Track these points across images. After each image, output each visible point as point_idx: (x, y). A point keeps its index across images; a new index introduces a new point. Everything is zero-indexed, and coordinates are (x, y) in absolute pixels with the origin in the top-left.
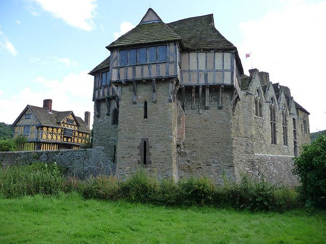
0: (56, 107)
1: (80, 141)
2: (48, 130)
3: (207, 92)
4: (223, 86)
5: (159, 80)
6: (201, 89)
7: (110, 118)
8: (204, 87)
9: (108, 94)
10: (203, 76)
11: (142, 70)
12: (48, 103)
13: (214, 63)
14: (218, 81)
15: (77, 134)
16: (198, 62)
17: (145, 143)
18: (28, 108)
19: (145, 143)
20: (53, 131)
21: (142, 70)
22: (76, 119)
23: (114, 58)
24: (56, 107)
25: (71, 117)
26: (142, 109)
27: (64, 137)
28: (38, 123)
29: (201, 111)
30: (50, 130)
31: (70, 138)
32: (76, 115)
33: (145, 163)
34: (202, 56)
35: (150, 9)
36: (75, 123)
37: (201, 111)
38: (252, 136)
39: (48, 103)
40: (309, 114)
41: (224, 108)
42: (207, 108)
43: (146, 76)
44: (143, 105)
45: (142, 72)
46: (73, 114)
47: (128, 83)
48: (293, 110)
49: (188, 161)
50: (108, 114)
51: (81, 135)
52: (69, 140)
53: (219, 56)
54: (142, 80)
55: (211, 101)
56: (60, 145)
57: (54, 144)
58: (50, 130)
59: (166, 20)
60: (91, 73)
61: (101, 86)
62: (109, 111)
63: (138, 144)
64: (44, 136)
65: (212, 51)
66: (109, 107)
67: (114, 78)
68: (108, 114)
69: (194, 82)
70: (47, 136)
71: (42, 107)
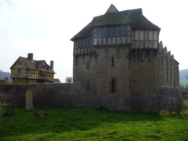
1: (49, 78)
2: (32, 71)
3: (144, 52)
4: (153, 49)
5: (121, 46)
6: (141, 50)
8: (143, 50)
9: (84, 52)
10: (142, 44)
11: (112, 39)
12: (30, 56)
13: (148, 37)
14: (150, 47)
15: (47, 74)
16: (139, 36)
17: (113, 80)
19: (113, 80)
20: (35, 72)
21: (112, 39)
22: (47, 65)
23: (95, 32)
24: (36, 58)
25: (44, 64)
26: (111, 61)
27: (41, 75)
28: (26, 67)
29: (139, 63)
30: (33, 71)
31: (44, 76)
32: (47, 63)
34: (142, 33)
35: (112, 5)
37: (139, 63)
38: (160, 76)
39: (30, 56)
40: (179, 64)
42: (142, 61)
43: (114, 43)
44: (111, 59)
45: (112, 41)
47: (103, 46)
48: (174, 63)
49: (133, 90)
50: (83, 64)
51: (51, 75)
52: (43, 77)
53: (151, 33)
54: (111, 45)
55: (144, 57)
58: (33, 71)
59: (119, 11)
60: (72, 40)
61: (79, 47)
62: (84, 62)
63: (109, 80)
64: (30, 75)
65: (147, 30)
66: (84, 59)
67: (95, 43)
68: (83, 64)
69: (137, 47)
70: (32, 75)
71: (27, 57)
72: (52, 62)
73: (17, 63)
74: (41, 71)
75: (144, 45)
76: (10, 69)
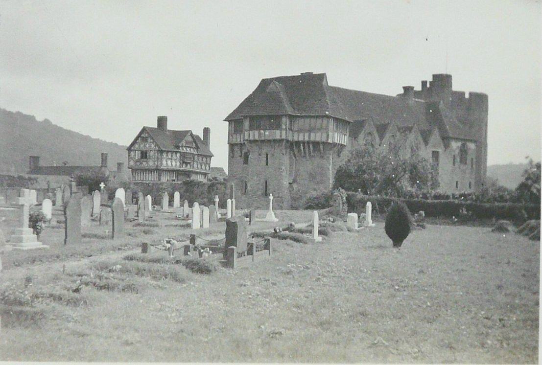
0: (171, 126)
2: (167, 156)
7: (242, 160)
8: (308, 142)
12: (162, 121)
18: (144, 130)
22: (195, 139)
24: (171, 126)
27: (184, 162)
33: (266, 195)
36: (194, 145)
39: (162, 121)
41: (325, 157)
46: (192, 135)
47: (255, 141)
50: (241, 156)
56: (178, 172)
57: (172, 171)
60: (225, 120)
64: (164, 162)
68: (241, 156)
72: (206, 131)
73: (140, 139)
74: (183, 155)
75: (309, 138)
76: (127, 151)
